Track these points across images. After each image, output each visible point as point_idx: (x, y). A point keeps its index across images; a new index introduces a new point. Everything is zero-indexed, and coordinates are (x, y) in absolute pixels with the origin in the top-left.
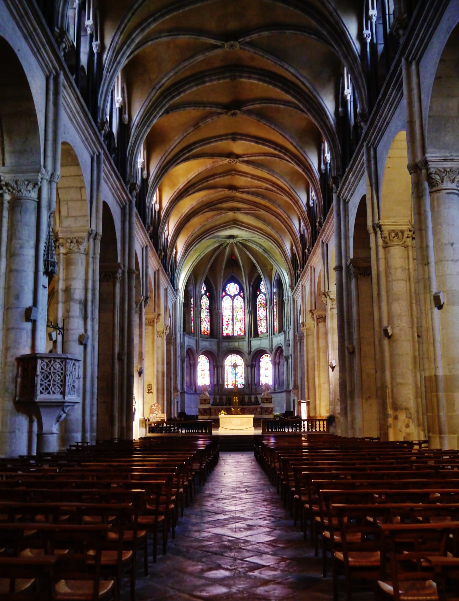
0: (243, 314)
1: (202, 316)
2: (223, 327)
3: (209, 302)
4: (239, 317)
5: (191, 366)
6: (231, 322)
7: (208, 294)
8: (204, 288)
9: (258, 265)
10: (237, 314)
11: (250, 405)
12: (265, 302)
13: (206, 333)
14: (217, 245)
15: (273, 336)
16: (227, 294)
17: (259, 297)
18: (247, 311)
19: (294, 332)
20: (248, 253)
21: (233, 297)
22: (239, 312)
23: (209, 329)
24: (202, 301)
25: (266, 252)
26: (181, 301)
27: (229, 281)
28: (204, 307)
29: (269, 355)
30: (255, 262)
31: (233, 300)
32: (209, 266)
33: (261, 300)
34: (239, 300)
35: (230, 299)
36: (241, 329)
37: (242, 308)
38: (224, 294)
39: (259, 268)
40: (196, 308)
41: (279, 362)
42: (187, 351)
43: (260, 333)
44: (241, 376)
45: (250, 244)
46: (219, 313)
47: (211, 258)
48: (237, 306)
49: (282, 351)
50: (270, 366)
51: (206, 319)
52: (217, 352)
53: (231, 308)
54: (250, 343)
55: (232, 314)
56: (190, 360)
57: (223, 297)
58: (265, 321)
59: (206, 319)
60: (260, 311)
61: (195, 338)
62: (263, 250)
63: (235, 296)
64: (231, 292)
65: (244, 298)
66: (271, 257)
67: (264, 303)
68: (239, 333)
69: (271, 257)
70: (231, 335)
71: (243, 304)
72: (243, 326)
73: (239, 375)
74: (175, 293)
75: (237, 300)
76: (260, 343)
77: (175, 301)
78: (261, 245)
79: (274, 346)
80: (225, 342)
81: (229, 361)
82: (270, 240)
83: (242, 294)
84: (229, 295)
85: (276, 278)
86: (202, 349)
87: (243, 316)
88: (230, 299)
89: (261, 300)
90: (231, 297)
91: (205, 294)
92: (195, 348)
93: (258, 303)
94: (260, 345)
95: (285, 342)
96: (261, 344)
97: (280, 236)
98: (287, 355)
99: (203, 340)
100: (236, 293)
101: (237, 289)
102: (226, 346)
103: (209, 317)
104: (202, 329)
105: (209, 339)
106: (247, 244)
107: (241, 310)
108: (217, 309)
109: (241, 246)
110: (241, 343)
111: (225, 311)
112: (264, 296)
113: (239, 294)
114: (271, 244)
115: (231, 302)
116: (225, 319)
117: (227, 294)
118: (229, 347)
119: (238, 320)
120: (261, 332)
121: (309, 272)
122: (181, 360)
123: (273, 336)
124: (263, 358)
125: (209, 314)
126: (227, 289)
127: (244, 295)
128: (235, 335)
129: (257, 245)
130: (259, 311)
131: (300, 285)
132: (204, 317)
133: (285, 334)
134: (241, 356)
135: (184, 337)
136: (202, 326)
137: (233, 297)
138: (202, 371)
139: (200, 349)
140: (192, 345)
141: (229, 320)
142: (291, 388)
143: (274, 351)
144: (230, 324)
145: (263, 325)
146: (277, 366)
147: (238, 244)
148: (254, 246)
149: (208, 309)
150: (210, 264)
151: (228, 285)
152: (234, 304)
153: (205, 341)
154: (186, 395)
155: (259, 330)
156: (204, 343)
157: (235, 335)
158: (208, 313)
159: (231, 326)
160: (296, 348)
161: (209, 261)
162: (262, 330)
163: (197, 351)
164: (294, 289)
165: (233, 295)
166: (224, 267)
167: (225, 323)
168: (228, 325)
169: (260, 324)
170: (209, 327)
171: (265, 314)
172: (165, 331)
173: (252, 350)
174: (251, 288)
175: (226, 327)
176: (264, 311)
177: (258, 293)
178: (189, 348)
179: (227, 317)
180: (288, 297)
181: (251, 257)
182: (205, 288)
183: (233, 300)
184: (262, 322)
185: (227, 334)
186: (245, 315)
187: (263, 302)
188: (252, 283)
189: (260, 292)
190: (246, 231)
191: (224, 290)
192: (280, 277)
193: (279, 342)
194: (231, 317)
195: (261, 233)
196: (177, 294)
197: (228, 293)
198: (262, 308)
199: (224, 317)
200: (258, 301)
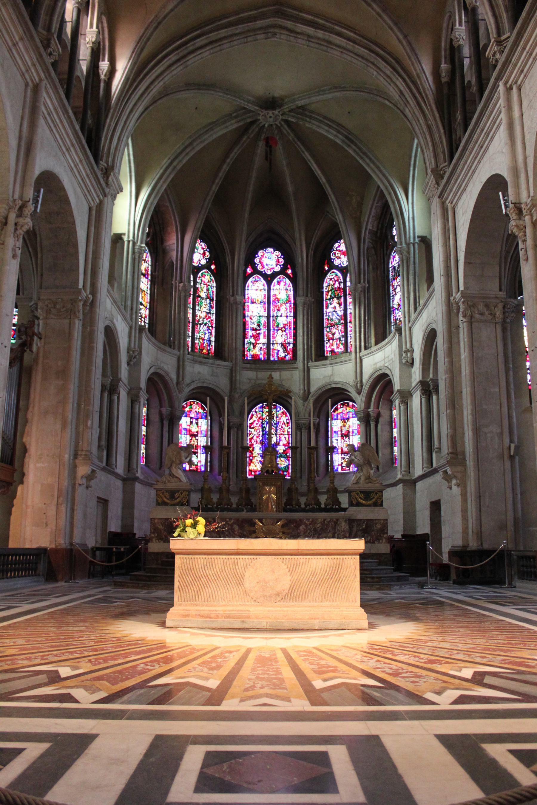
0: (292, 314)
1: (198, 313)
2: (246, 341)
3: (214, 285)
4: (282, 321)
5: (162, 420)
6: (263, 330)
7: (213, 267)
8: (204, 254)
9: (331, 188)
10: (279, 314)
11: (313, 510)
12: (342, 285)
13: (204, 351)
14: (233, 125)
15: (364, 352)
16: (256, 271)
17: (329, 276)
18: (300, 300)
19: (449, 294)
20: (307, 156)
21: (269, 279)
22: (283, 309)
23: (213, 344)
24: (199, 281)
25: (352, 142)
26: (137, 247)
27: (264, 247)
28: (203, 295)
29: (351, 403)
30: (323, 180)
31: (269, 283)
32: (215, 188)
33: (332, 283)
34: (282, 284)
35: (262, 283)
36: (284, 346)
37: (288, 301)
38: (249, 271)
39: (332, 198)
40: (181, 285)
41: (379, 415)
42: (150, 380)
43: (329, 354)
44: (285, 452)
45: (313, 126)
46: (236, 303)
47: (220, 168)
48: (278, 297)
49: (389, 383)
50: (354, 423)
51: (206, 321)
52: (227, 390)
53: (266, 300)
54: (307, 372)
55: (266, 314)
56: (161, 406)
57: (247, 277)
58: (340, 326)
59: (206, 321)
60: (330, 306)
61: (176, 352)
62: (347, 137)
63: (275, 275)
64: (266, 267)
65: (294, 280)
66: (365, 154)
67: (339, 288)
68: (282, 354)
69: (365, 154)
70: (261, 357)
71: (291, 293)
72: (291, 340)
73: (280, 449)
74: (102, 182)
75: (279, 283)
76: (330, 373)
77: (101, 202)
78: (339, 125)
79: (365, 377)
80: (247, 369)
81: (254, 418)
82: (372, 57)
83: (289, 271)
84: (260, 273)
85: (370, 227)
86: (193, 382)
87: (291, 319)
88: (264, 282)
89: (332, 283)
90: (265, 276)
91: (207, 266)
92: (174, 376)
93: (325, 290)
94: (330, 376)
95: (400, 355)
96: (332, 375)
97: (405, 37)
98: (405, 388)
99: (194, 361)
100: (277, 269)
101: (278, 261)
102: (250, 379)
103: (213, 317)
104: (197, 341)
105: (211, 361)
106: (307, 125)
107: (288, 305)
108: (233, 295)
109: (291, 137)
110: (286, 374)
111: (251, 306)
112: (339, 275)
113: (283, 272)
114: (375, 73)
115: (266, 288)
116: (251, 324)
117: (256, 271)
118: (259, 382)
119: (281, 326)
120: (332, 351)
121: (502, 102)
122: (128, 393)
123: (364, 352)
124: (336, 409)
125: (214, 311)
126: (257, 260)
127: (294, 272)
128: (272, 359)
129: (330, 126)
130: (327, 307)
131: (501, 88)
132: (203, 315)
133: (400, 334)
134: (284, 407)
135: (140, 338)
136: (197, 335)
137: (269, 279)
138: (193, 435)
139: (187, 380)
140: (166, 368)
141: (259, 325)
142: (418, 470)
143: (366, 388)
144: (262, 336)
145: (337, 336)
146: (372, 425)
147: (286, 129)
148: (323, 130)
149: (212, 300)
150: (218, 181)
151: (260, 253)
152: (272, 293)
153: (201, 363)
154: (137, 484)
155: (328, 347)
156: (198, 368)
157: (272, 359)
158: (211, 307)
159: (263, 340)
160: (455, 340)
161: (216, 176)
162: (334, 347)
163: (178, 383)
164: (442, 178)
165: (269, 273)
166: (250, 195)
167: (250, 333)
168: (256, 337)
169: (330, 336)
170: (213, 339)
171: (341, 313)
172: (12, 217)
173: (313, 390)
174: (311, 253)
175: (253, 340)
176: (340, 304)
177: (326, 268)
178: (155, 373)
179: (255, 320)
180: (408, 245)
181: (314, 166)
182: (207, 253)
183: (269, 283)
184: (334, 331)
185: (253, 356)
186: (295, 317)
187: (337, 285)
188: (314, 242)
189: (332, 266)
190: (309, 37)
191: (250, 261)
192: (387, 201)
193: (379, 365)
194: (263, 320)
195: (349, 39)
196: (107, 183)
197: (259, 267)
198: (336, 300)
199: (247, 319)
200: (325, 285)
